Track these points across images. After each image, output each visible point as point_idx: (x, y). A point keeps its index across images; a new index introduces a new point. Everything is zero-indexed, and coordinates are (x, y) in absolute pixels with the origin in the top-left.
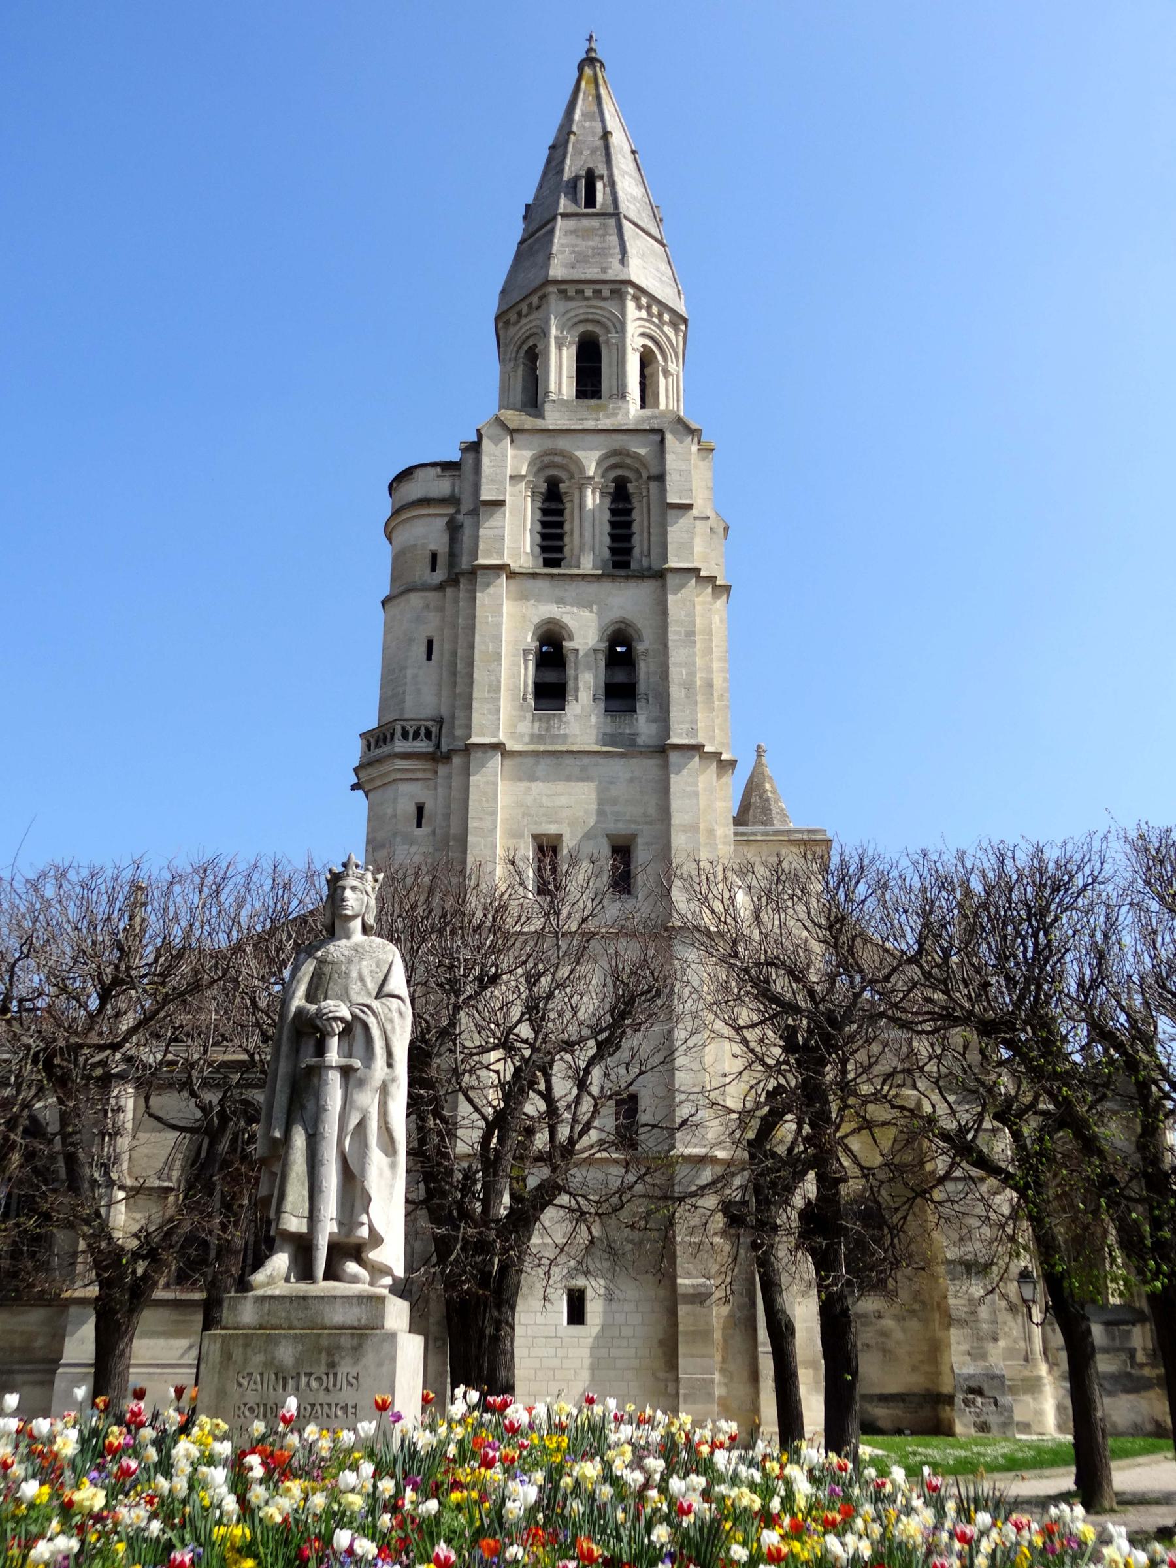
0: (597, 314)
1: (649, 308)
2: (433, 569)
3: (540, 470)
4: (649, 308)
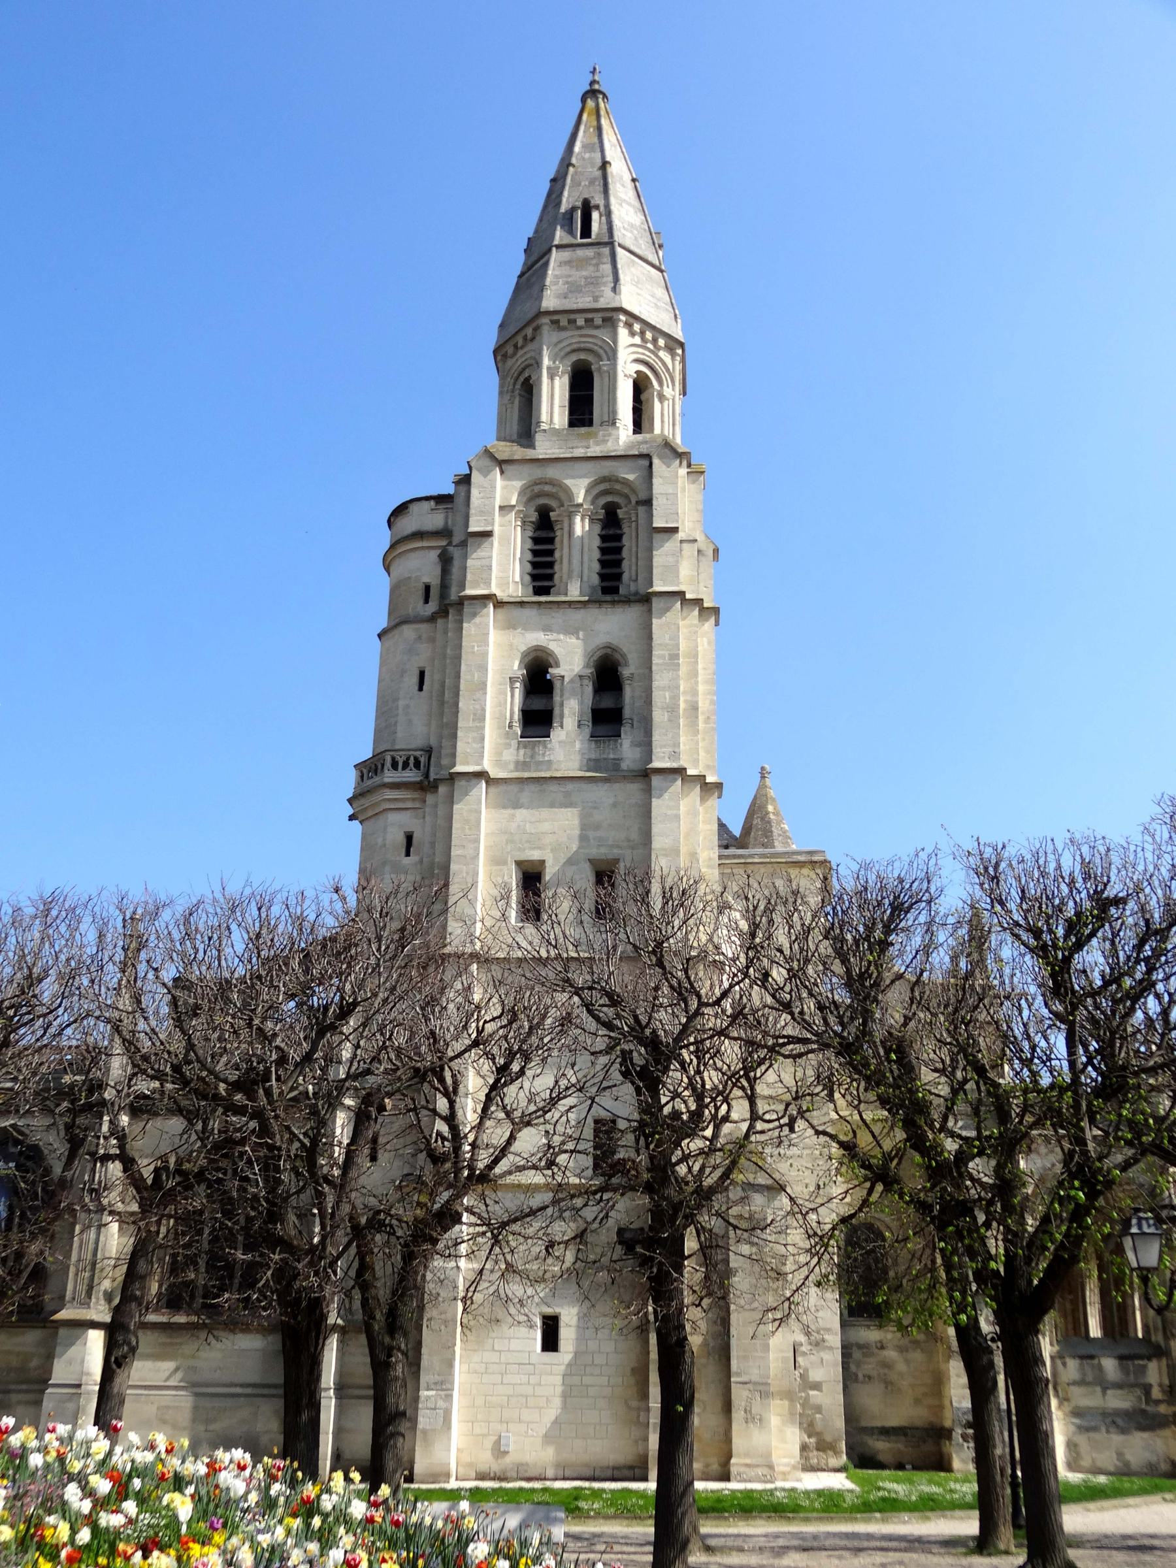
0: (589, 342)
1: (642, 333)
2: (426, 601)
3: (530, 499)
4: (642, 333)
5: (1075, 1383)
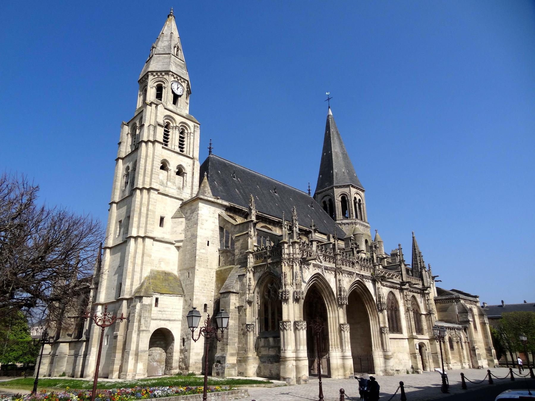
1: (157, 74)
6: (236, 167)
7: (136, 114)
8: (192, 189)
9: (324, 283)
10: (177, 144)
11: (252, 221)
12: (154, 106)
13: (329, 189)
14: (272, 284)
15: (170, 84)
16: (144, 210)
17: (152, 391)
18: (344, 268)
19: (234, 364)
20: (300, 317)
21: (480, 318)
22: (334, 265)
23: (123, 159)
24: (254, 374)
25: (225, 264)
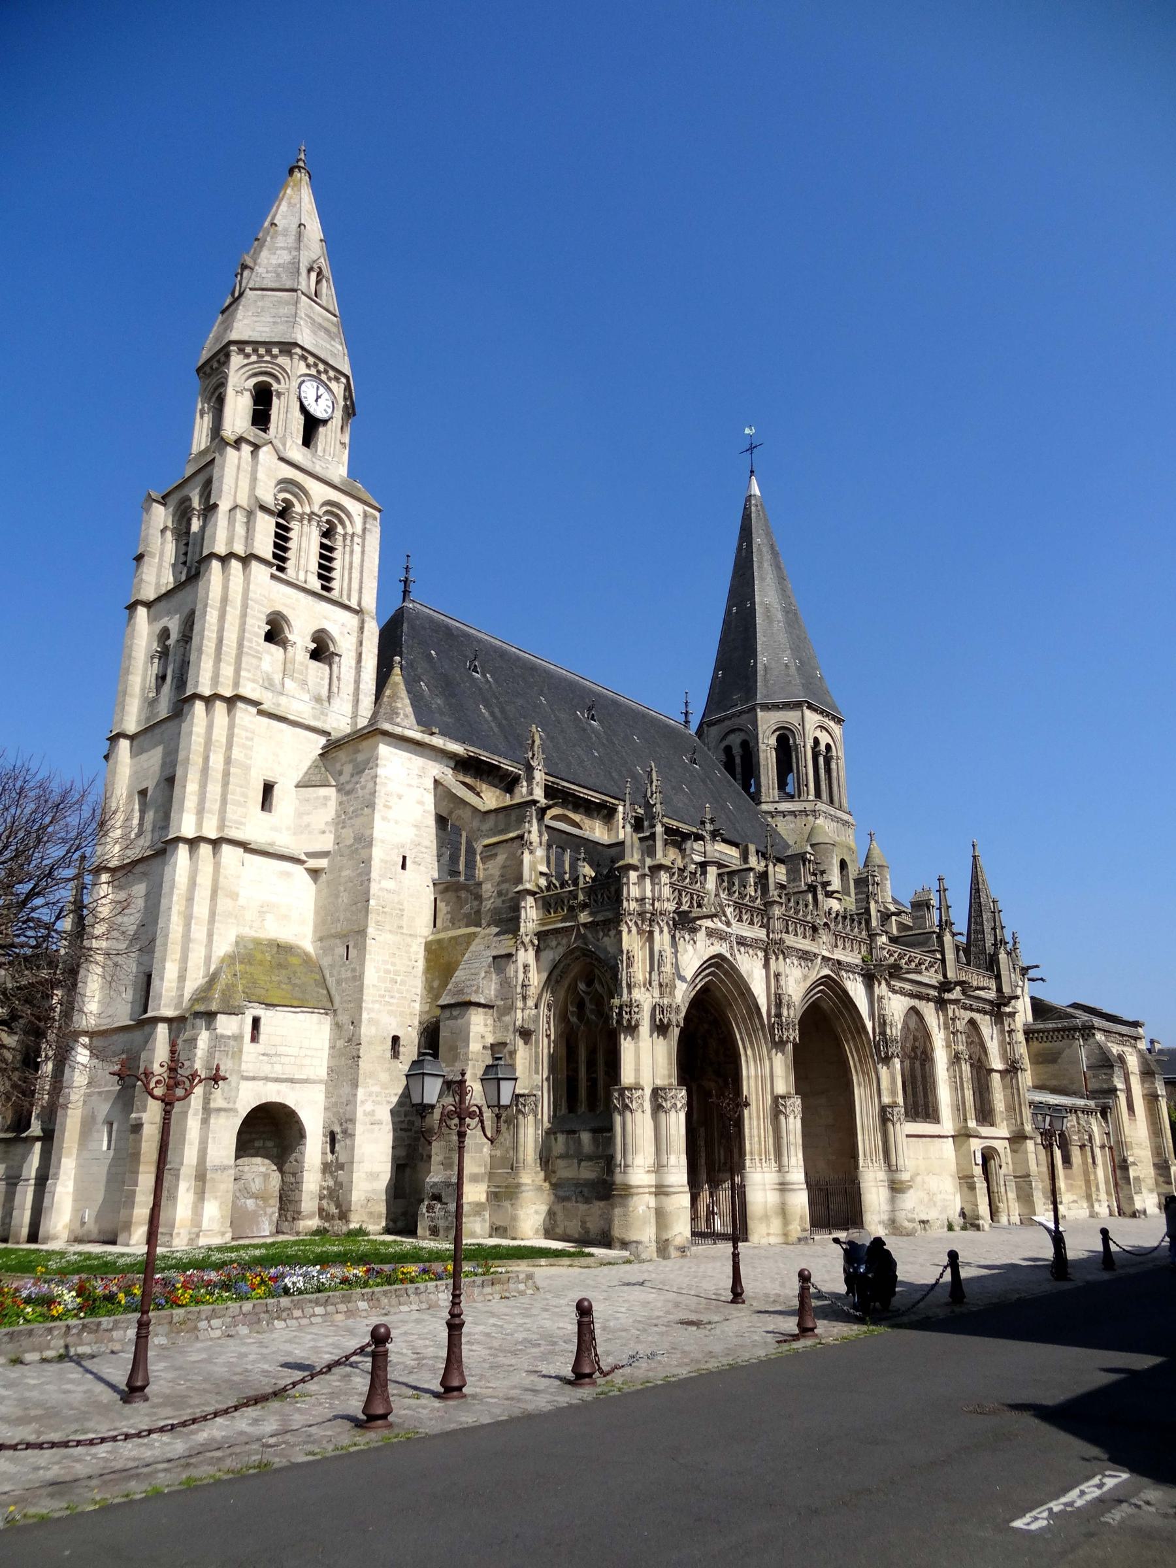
1: (255, 351)
5: (561, 1157)
6: (479, 641)
7: (189, 472)
8: (356, 702)
9: (735, 983)
10: (314, 567)
11: (535, 802)
12: (246, 449)
13: (741, 713)
14: (589, 984)
15: (295, 384)
16: (217, 760)
17: (274, 1279)
18: (790, 940)
19: (479, 1204)
20: (670, 1077)
21: (1143, 1082)
22: (764, 931)
23: (148, 605)
24: (537, 1232)
25: (453, 922)
